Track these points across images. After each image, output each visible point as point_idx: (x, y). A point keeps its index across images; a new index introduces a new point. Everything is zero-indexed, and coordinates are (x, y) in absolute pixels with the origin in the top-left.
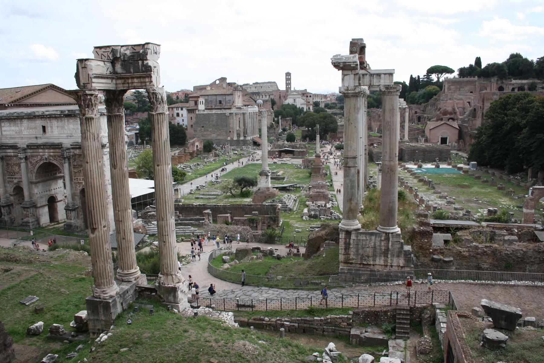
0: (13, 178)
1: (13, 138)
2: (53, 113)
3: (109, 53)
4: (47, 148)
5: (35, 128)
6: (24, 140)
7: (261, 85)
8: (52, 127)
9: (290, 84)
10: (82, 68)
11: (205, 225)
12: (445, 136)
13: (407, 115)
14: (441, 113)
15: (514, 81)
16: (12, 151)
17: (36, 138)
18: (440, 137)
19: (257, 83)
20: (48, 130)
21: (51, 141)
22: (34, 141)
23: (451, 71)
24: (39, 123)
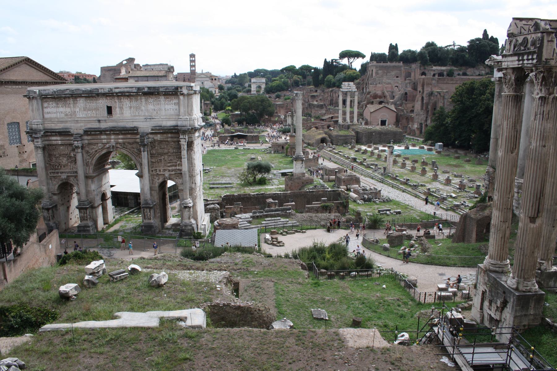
0: (58, 173)
1: (62, 122)
2: (126, 90)
3: (531, 26)
4: (114, 134)
5: (97, 109)
6: (79, 125)
7: (152, 67)
8: (121, 108)
9: (194, 66)
10: (548, 41)
11: (292, 215)
12: (385, 119)
13: (356, 98)
14: (371, 96)
15: (434, 68)
16: (58, 138)
17: (99, 121)
18: (380, 120)
19: (147, 65)
20: (116, 111)
21: (121, 124)
22: (96, 125)
23: (363, 57)
24: (103, 103)
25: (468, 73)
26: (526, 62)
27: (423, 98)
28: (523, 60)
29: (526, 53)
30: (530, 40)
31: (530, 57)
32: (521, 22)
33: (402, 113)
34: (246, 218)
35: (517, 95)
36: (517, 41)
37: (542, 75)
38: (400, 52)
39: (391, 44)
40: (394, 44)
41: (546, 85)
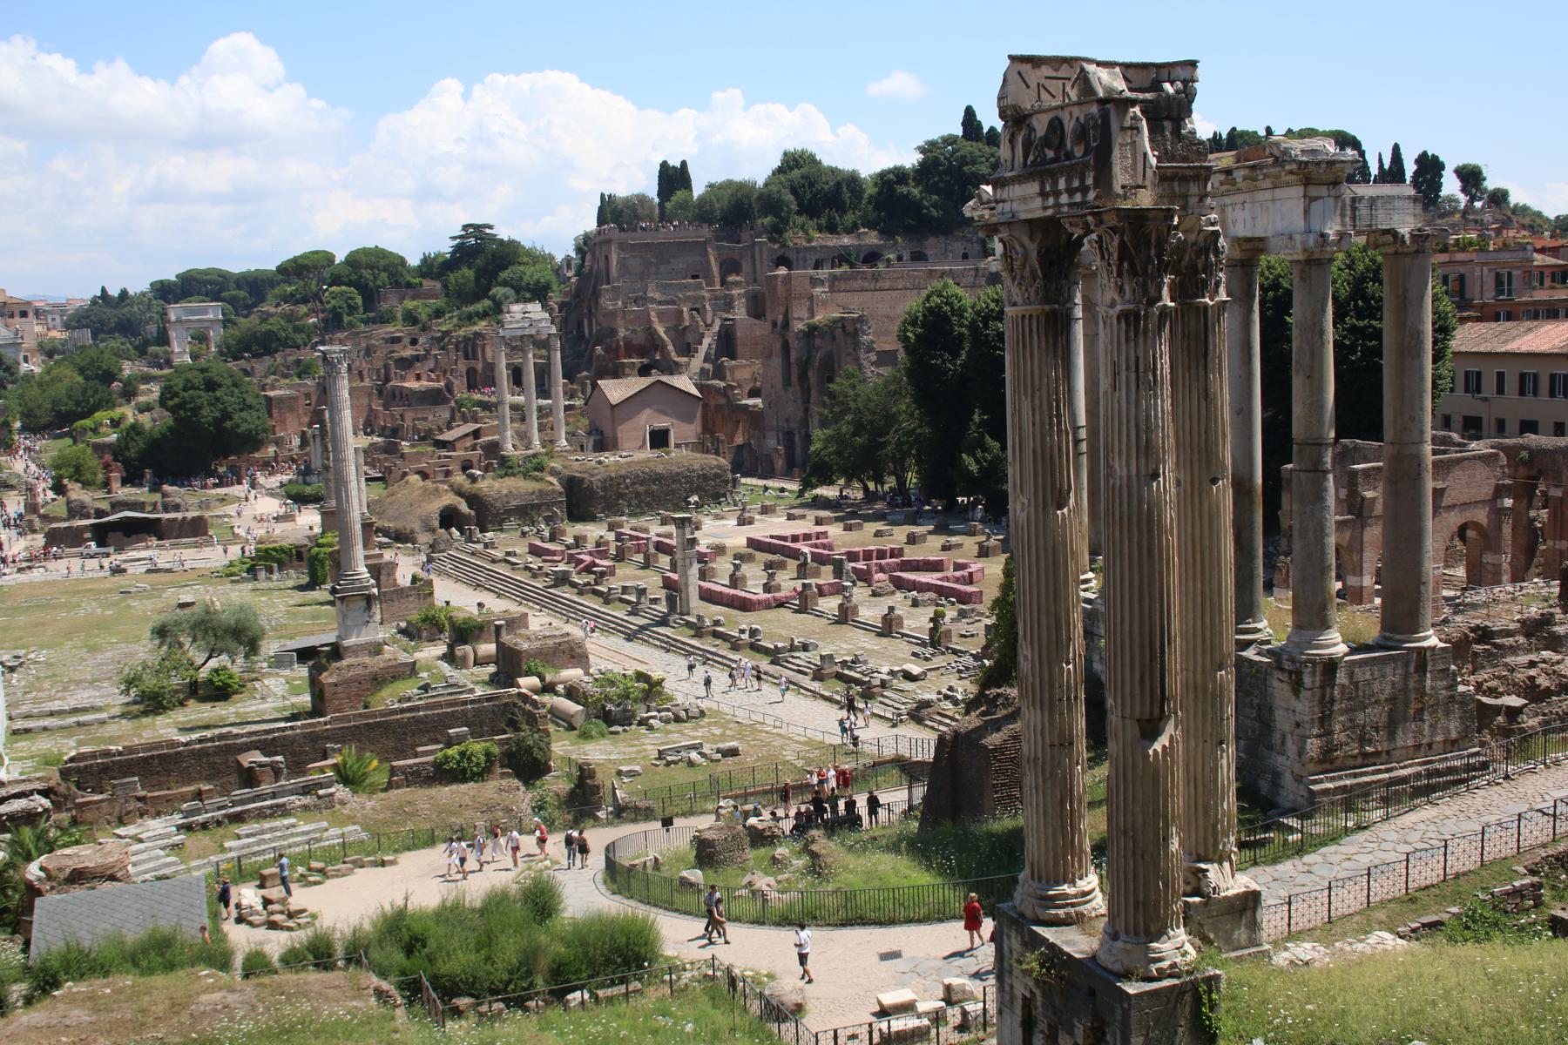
25: (929, 252)
26: (1064, 199)
27: (786, 348)
28: (1057, 194)
29: (1061, 171)
30: (1069, 126)
31: (1076, 184)
32: (1037, 72)
33: (723, 401)
34: (160, 837)
35: (1054, 312)
36: (1032, 129)
37: (1116, 238)
38: (698, 189)
39: (664, 165)
40: (675, 162)
41: (1133, 272)
